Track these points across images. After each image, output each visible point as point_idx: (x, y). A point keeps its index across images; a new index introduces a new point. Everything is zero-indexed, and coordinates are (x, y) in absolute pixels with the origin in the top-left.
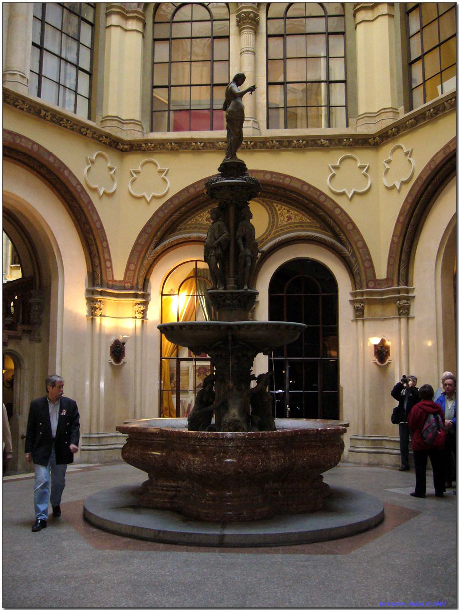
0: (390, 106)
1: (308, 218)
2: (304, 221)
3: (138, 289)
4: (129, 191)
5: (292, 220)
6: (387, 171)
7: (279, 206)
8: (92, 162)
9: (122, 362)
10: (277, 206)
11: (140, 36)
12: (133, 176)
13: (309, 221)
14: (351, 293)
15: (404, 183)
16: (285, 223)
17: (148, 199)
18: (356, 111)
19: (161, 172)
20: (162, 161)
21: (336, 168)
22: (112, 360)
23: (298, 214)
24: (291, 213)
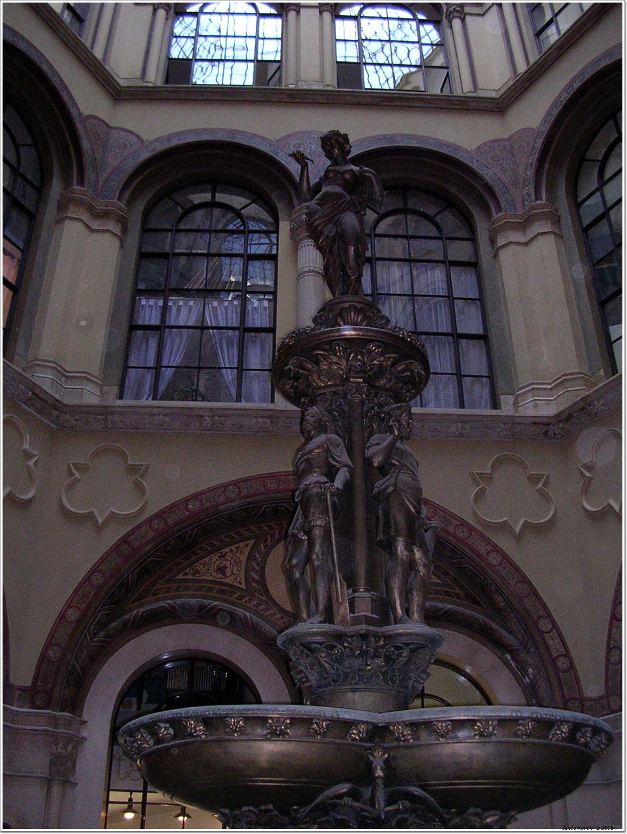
4: (62, 504)
11: (117, 243)
12: (72, 474)
21: (487, 478)
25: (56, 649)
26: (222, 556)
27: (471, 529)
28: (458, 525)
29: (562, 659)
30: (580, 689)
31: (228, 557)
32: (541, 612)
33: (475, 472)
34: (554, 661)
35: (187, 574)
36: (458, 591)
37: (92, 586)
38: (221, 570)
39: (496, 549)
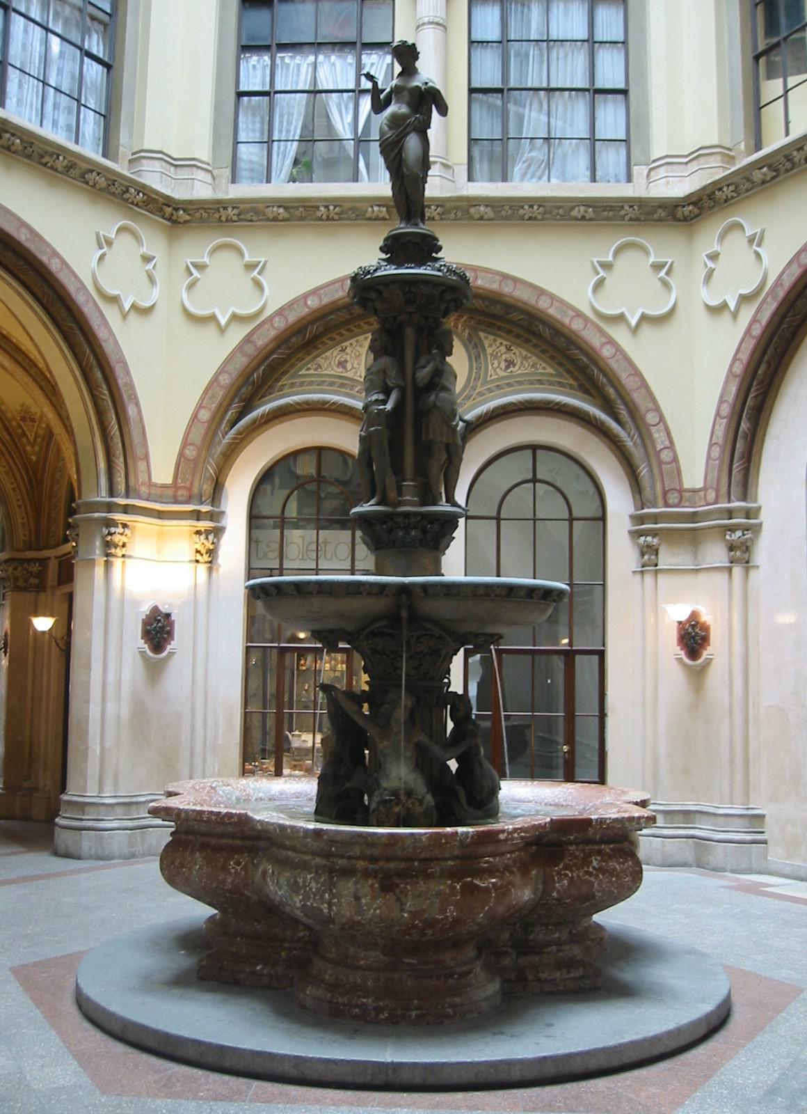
0: (715, 142)
1: (550, 365)
2: (542, 371)
3: (201, 503)
5: (517, 367)
6: (710, 275)
7: (491, 337)
8: (109, 243)
9: (168, 650)
10: (486, 338)
13: (550, 370)
14: (632, 517)
15: (744, 299)
16: (502, 374)
17: (223, 321)
18: (646, 149)
19: (250, 267)
20: (255, 246)
21: (607, 266)
22: (146, 646)
23: (529, 355)
24: (514, 353)
25: (191, 448)
26: (343, 350)
27: (586, 320)
28: (574, 316)
29: (666, 452)
30: (680, 480)
31: (348, 350)
32: (651, 405)
33: (595, 260)
34: (658, 454)
35: (308, 369)
36: (572, 382)
37: (220, 386)
38: (342, 364)
39: (611, 342)
